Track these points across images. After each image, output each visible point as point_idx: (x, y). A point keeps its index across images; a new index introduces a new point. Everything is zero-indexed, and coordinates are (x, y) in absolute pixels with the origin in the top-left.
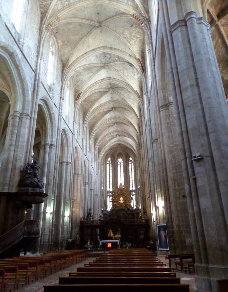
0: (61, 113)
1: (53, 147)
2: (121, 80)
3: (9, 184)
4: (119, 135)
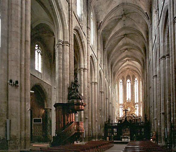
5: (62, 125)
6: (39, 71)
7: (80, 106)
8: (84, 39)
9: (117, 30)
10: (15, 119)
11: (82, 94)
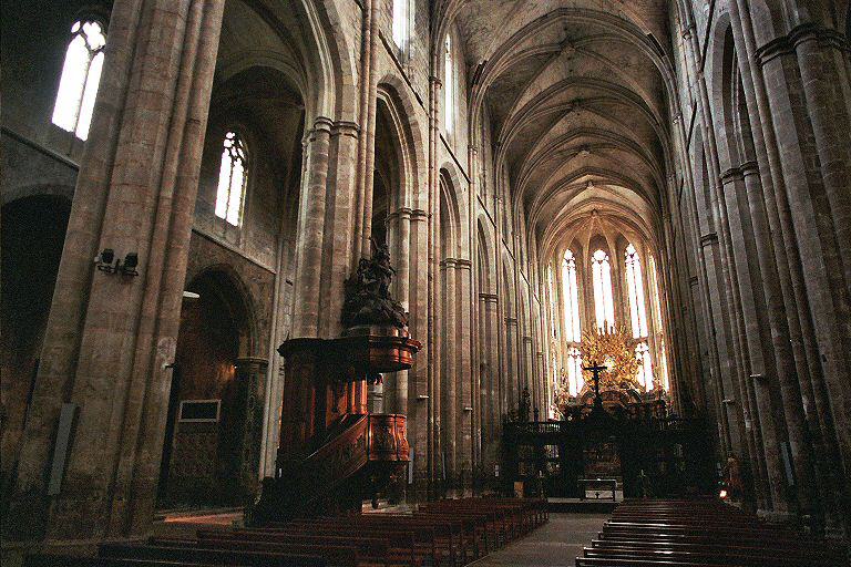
0: (436, 121)
1: (420, 218)
2: (600, 9)
3: (319, 317)
4: (595, 183)
5: (308, 429)
6: (229, 220)
7: (396, 351)
8: (417, 117)
9: (544, 88)
10: (101, 402)
11: (406, 306)
